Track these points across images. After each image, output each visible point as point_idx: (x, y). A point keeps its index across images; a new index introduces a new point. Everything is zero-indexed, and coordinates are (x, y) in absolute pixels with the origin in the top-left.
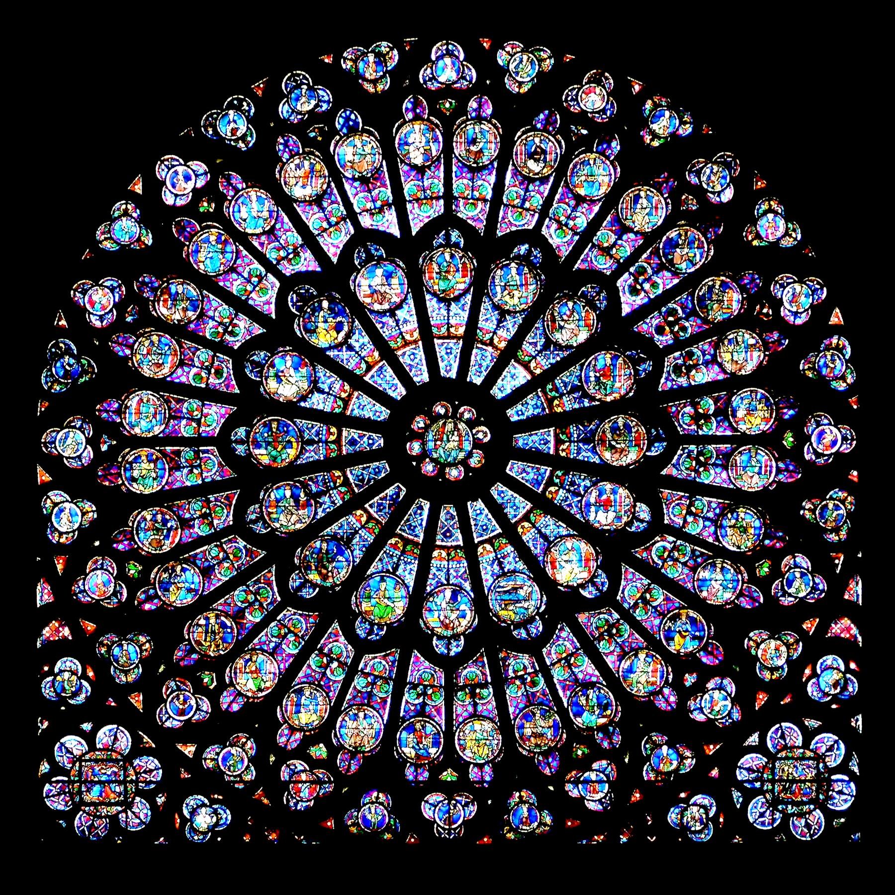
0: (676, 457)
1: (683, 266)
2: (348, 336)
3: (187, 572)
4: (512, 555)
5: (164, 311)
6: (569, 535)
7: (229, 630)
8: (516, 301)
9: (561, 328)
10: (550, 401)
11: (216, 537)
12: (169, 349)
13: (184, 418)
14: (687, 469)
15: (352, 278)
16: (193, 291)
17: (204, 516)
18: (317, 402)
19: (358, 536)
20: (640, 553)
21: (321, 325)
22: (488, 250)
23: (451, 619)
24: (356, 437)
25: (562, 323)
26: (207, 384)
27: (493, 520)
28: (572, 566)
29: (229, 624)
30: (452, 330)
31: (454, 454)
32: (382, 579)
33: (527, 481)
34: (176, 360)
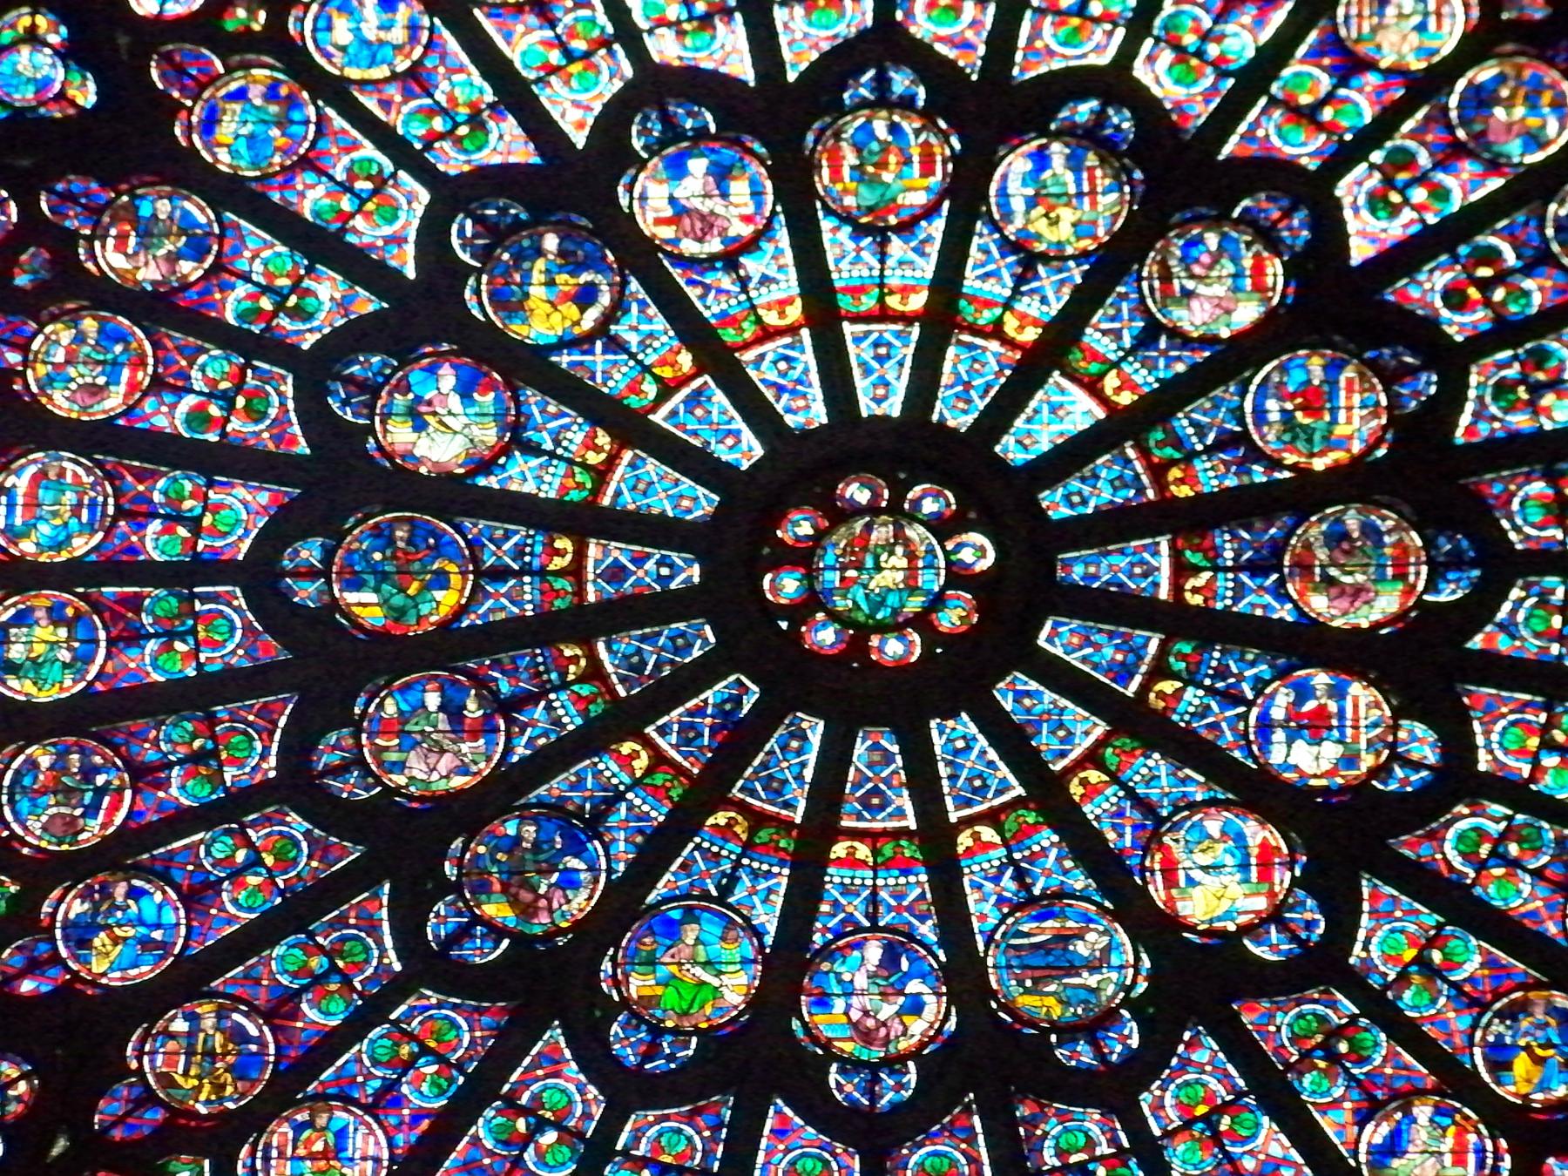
0: (1506, 607)
1: (1514, 149)
2: (609, 317)
3: (144, 902)
4: (1054, 852)
5: (119, 261)
6: (1212, 803)
7: (254, 1048)
8: (1064, 231)
9: (1188, 294)
10: (1158, 472)
11: (229, 810)
12: (126, 350)
13: (154, 515)
14: (1537, 635)
15: (625, 180)
16: (199, 212)
17: (196, 759)
18: (522, 476)
19: (623, 806)
20: (1408, 847)
21: (537, 292)
22: (989, 111)
23: (882, 1017)
24: (624, 560)
25: (1190, 285)
26: (224, 435)
27: (1001, 764)
28: (1220, 881)
29: (253, 1031)
30: (893, 302)
31: (892, 600)
32: (690, 915)
33: (1096, 667)
34: (144, 379)
